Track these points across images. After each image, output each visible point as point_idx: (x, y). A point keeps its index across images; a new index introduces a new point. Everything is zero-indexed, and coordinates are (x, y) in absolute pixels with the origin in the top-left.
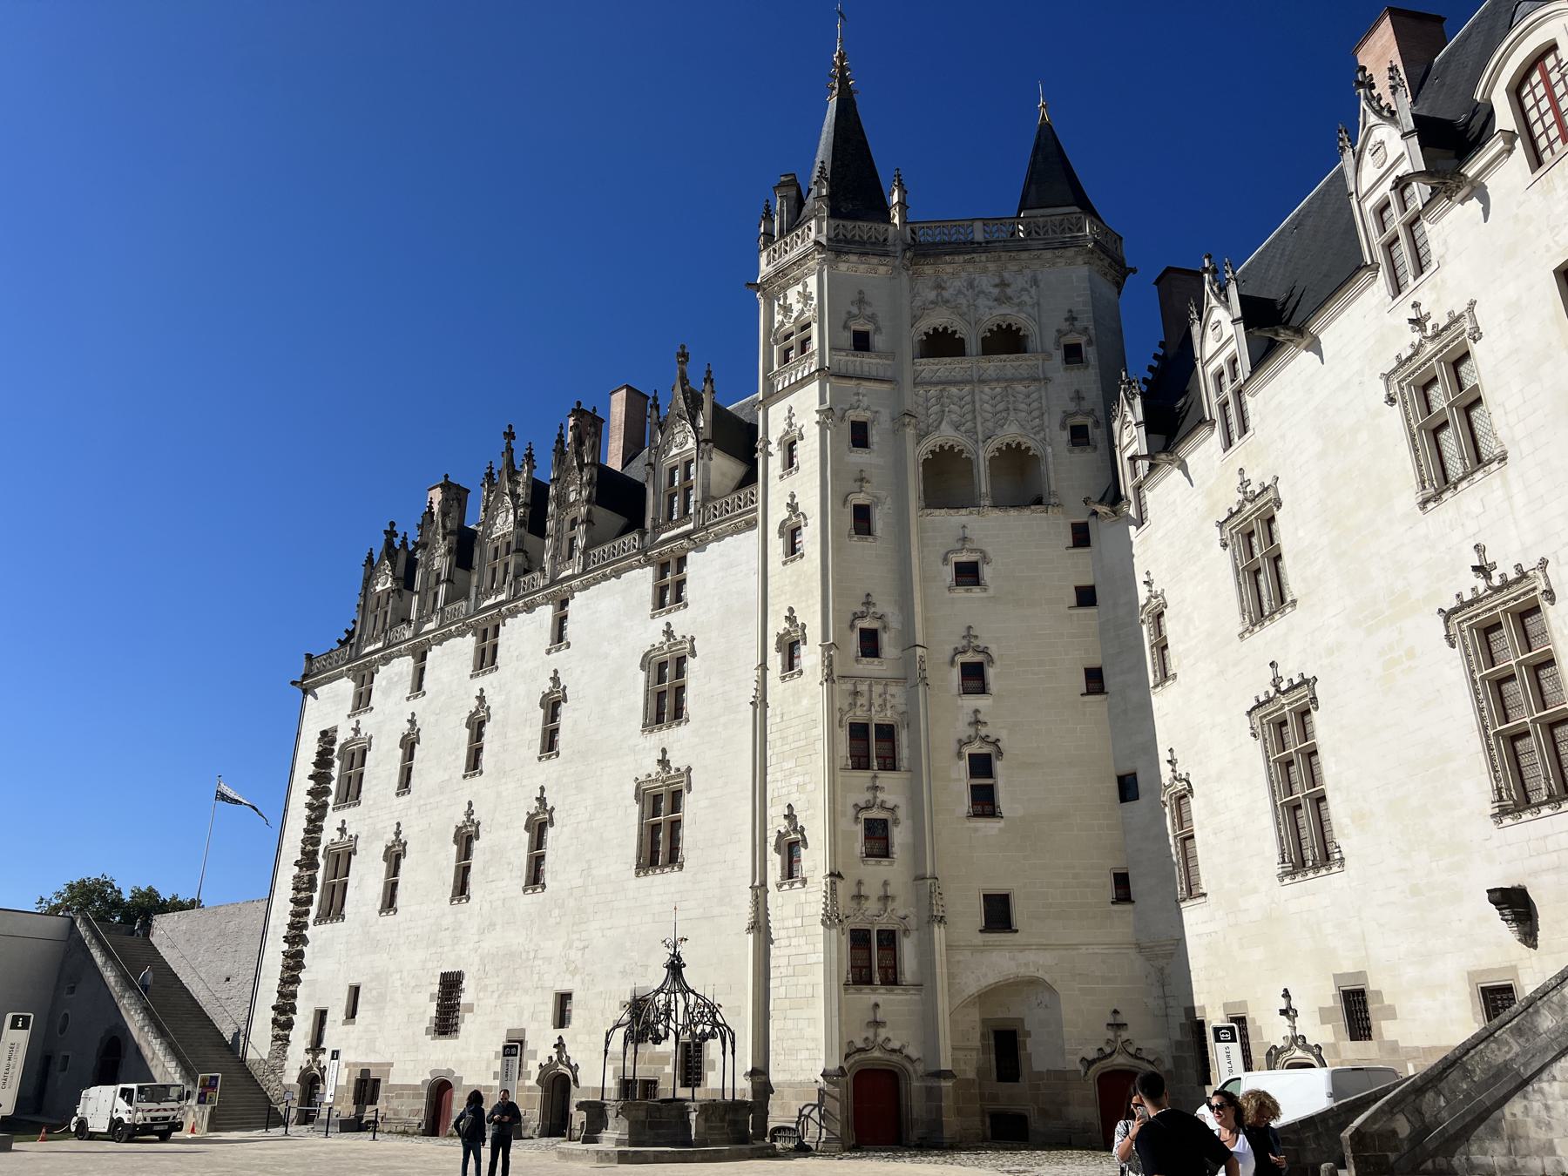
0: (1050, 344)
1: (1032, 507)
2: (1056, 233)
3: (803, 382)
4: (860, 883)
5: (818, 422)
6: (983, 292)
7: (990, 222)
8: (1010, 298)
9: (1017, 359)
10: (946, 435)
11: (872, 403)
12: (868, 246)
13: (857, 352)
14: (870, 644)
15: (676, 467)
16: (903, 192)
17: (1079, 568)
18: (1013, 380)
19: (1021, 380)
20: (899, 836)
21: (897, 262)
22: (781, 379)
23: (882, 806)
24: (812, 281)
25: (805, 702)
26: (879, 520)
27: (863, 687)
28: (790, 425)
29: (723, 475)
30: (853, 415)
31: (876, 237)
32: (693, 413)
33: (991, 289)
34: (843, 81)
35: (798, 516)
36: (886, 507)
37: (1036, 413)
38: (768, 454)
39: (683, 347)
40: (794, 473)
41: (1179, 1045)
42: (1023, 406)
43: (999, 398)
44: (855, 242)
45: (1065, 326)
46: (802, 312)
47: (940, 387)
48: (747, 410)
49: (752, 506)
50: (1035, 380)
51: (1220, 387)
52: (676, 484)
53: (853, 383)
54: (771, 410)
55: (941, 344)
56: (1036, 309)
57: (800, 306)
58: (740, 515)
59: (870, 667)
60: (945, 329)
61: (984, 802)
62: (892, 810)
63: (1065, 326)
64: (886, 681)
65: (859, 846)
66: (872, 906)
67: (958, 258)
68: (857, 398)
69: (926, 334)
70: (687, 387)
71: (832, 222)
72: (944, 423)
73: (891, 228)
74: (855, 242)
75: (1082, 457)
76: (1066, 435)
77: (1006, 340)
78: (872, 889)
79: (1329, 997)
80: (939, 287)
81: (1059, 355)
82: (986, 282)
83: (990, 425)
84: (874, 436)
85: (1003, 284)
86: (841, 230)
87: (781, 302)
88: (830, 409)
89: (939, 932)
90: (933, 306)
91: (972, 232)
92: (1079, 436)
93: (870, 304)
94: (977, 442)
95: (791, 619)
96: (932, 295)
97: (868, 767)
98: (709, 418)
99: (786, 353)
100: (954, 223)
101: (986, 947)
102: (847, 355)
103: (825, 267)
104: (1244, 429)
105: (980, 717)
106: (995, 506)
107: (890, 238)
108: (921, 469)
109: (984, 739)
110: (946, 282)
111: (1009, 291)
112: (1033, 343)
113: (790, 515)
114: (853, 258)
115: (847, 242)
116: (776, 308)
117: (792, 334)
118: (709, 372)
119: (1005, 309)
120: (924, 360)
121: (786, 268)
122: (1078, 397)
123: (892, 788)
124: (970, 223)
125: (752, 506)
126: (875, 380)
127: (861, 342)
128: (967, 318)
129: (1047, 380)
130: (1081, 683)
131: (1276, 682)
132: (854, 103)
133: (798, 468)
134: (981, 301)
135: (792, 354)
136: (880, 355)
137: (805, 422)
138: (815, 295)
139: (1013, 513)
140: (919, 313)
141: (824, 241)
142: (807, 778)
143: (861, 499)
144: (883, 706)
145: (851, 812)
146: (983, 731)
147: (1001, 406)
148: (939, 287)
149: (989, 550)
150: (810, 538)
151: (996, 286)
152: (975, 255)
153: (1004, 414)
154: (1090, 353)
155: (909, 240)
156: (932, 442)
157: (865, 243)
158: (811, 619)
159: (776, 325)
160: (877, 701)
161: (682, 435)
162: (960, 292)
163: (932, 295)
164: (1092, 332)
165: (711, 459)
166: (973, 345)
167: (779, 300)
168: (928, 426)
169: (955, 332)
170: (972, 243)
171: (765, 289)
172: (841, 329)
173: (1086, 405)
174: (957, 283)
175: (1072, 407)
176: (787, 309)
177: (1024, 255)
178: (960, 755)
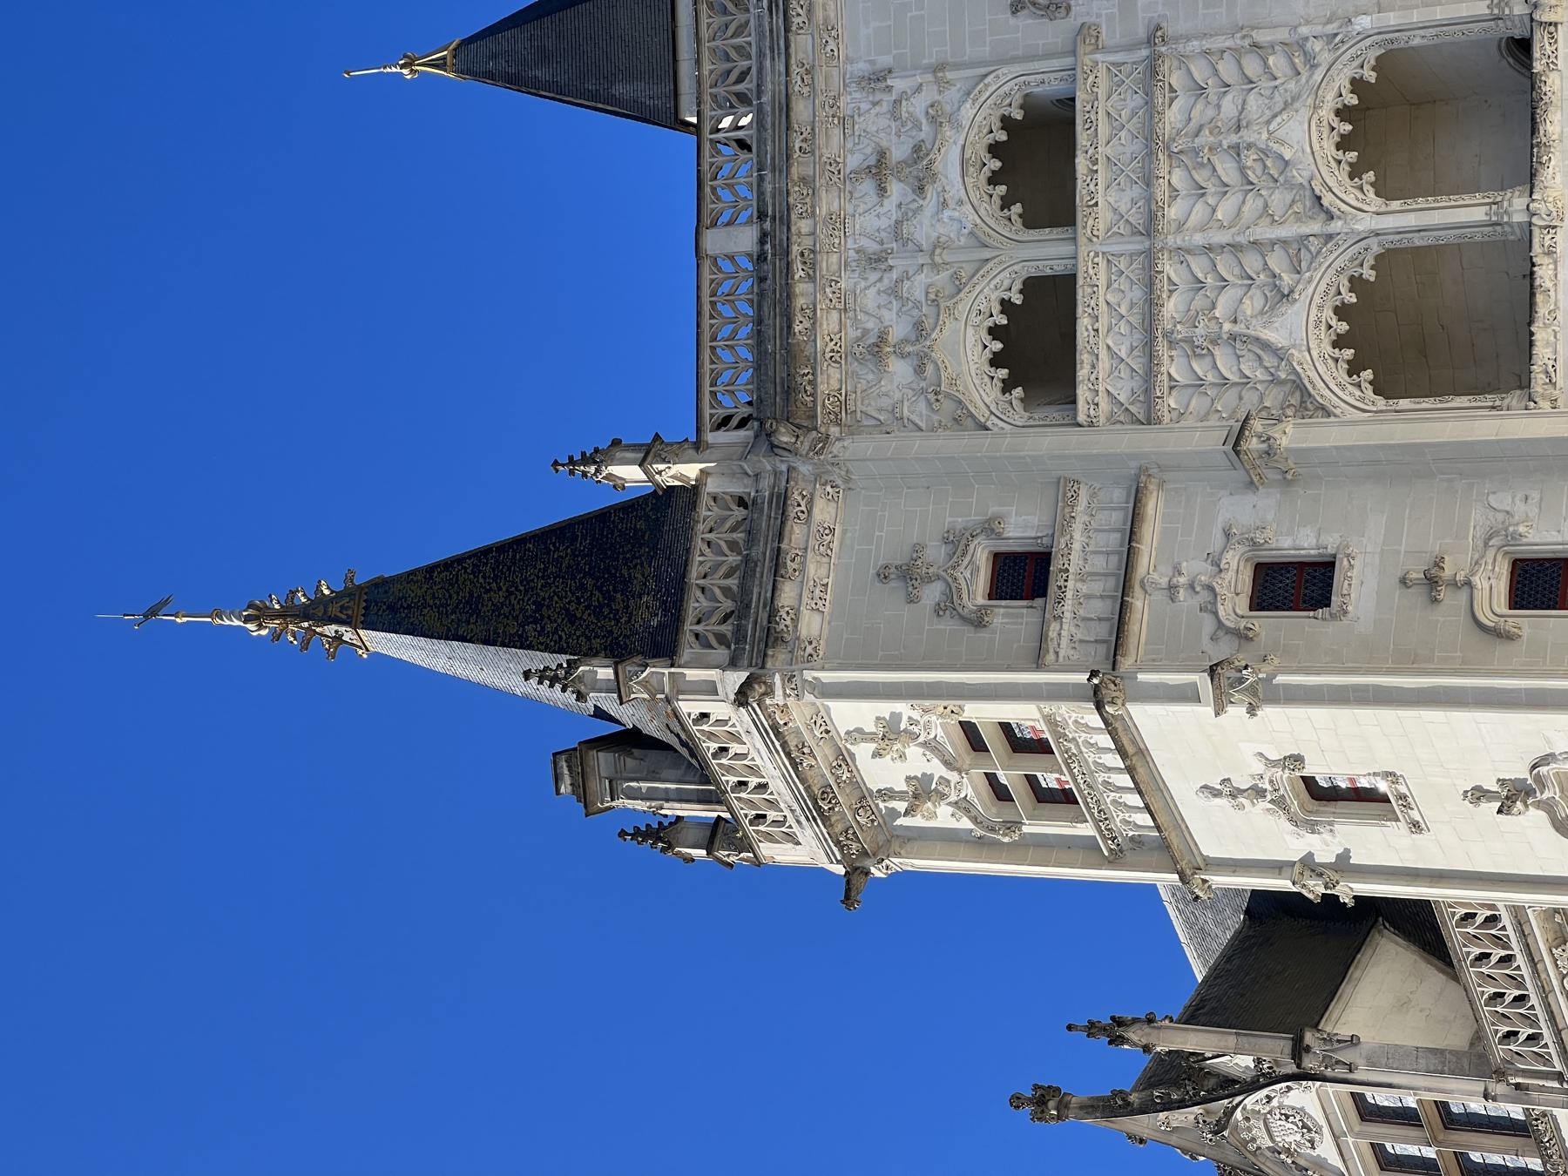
1: (1538, 67)
2: (747, 22)
3: (1130, 750)
5: (1252, 710)
6: (898, 223)
7: (709, 206)
8: (917, 149)
9: (1091, 124)
12: (756, 552)
13: (1052, 589)
15: (1378, 1150)
16: (614, 449)
18: (1151, 140)
19: (1151, 112)
21: (805, 469)
22: (1118, 817)
24: (848, 715)
28: (1261, 793)
29: (1403, 1005)
30: (1234, 601)
31: (733, 529)
32: (1211, 1083)
33: (890, 204)
34: (319, 611)
35: (1539, 780)
36: (1520, 508)
37: (1252, 66)
38: (1343, 865)
39: (1017, 1101)
40: (1403, 789)
42: (1229, 107)
43: (1201, 176)
44: (744, 589)
46: (932, 746)
47: (1162, 348)
48: (1207, 919)
49: (1506, 920)
50: (1152, 70)
52: (1429, 1152)
53: (1138, 602)
54: (1210, 849)
56: (949, 75)
58: (1533, 962)
60: (994, 332)
67: (802, 289)
68: (1182, 594)
69: (1007, 387)
70: (1133, 1098)
71: (686, 654)
72: (1268, 335)
73: (712, 486)
74: (744, 589)
80: (877, 349)
83: (1278, 200)
85: (879, 170)
86: (709, 628)
87: (901, 806)
88: (1212, 671)
90: (930, 368)
91: (731, 258)
93: (918, 548)
94: (1330, 237)
96: (900, 370)
98: (1228, 1038)
99: (1044, 796)
100: (707, 308)
102: (1059, 618)
103: (809, 675)
106: (1529, 178)
107: (737, 488)
108: (1404, 403)
110: (866, 332)
111: (899, 152)
112: (1049, 86)
113: (1539, 805)
114: (787, 594)
115: (742, 610)
116: (917, 821)
117: (992, 779)
118: (1092, 1028)
119: (948, 162)
120: (1083, 393)
121: (808, 789)
124: (707, 264)
125: (1506, 920)
126: (1132, 535)
128: (970, 268)
132: (380, 584)
133: (1390, 776)
134: (923, 229)
135: (1049, 780)
136: (1060, 523)
137: (1248, 750)
138: (885, 708)
141: (737, 678)
143: (1493, 585)
147: (1226, 169)
148: (877, 349)
151: (882, 190)
152: (795, 249)
153: (1250, 158)
155: (745, 434)
157: (747, 560)
159: (966, 823)
161: (1277, 1124)
162: (894, 292)
163: (900, 370)
165: (1354, 1041)
167: (894, 814)
168: (1275, 381)
169: (1006, 306)
170: (761, 257)
171: (864, 853)
172: (984, 634)
174: (870, 299)
176: (922, 792)
177: (801, 111)
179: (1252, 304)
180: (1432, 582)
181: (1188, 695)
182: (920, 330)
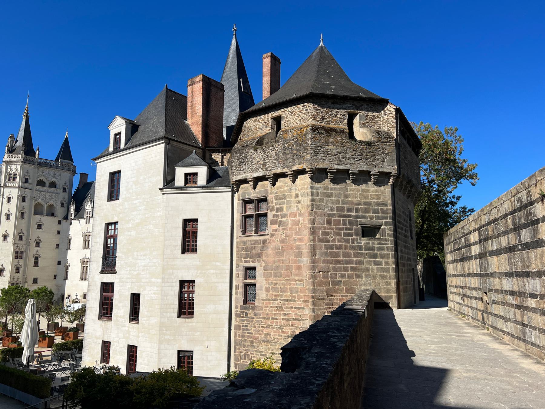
0: (61, 187)
4: (14, 277)
10: (40, 201)
11: (28, 193)
14: (21, 238)
16: (39, 151)
17: (58, 228)
20: (21, 269)
21: (36, 166)
23: (19, 265)
25: (8, 247)
26: (25, 216)
27: (19, 246)
28: (10, 194)
30: (23, 195)
34: (27, 114)
41: (59, 298)
45: (64, 184)
46: (15, 172)
50: (57, 194)
51: (87, 214)
55: (41, 183)
57: (15, 170)
59: (21, 242)
61: (36, 264)
62: (21, 265)
63: (64, 184)
64: (22, 244)
65: (15, 271)
66: (15, 280)
75: (63, 209)
76: (60, 204)
77: (53, 185)
78: (16, 278)
79: (82, 295)
80: (43, 172)
81: (62, 189)
82: (52, 173)
83: (48, 200)
84: (27, 200)
89: (26, 284)
92: (63, 205)
95: (6, 232)
96: (41, 173)
97: (17, 259)
101: (33, 286)
104: (89, 223)
105: (38, 251)
109: (38, 254)
111: (55, 176)
112: (57, 186)
115: (27, 161)
122: (64, 198)
123: (21, 262)
127: (26, 181)
129: (59, 194)
130: (55, 246)
131: (85, 257)
134: (50, 177)
139: (49, 217)
140: (38, 176)
142: (7, 260)
143: (23, 211)
144: (22, 249)
145: (14, 266)
146: (38, 253)
149: (44, 223)
150: (13, 218)
154: (67, 190)
156: (36, 202)
158: (11, 232)
159: (8, 171)
160: (21, 248)
163: (41, 173)
164: (68, 186)
166: (47, 185)
173: (65, 200)
175: (62, 200)
176: (11, 169)
178: (33, 257)
179: (42, 198)
180: (24, 208)
181: (18, 193)
182: (44, 175)
